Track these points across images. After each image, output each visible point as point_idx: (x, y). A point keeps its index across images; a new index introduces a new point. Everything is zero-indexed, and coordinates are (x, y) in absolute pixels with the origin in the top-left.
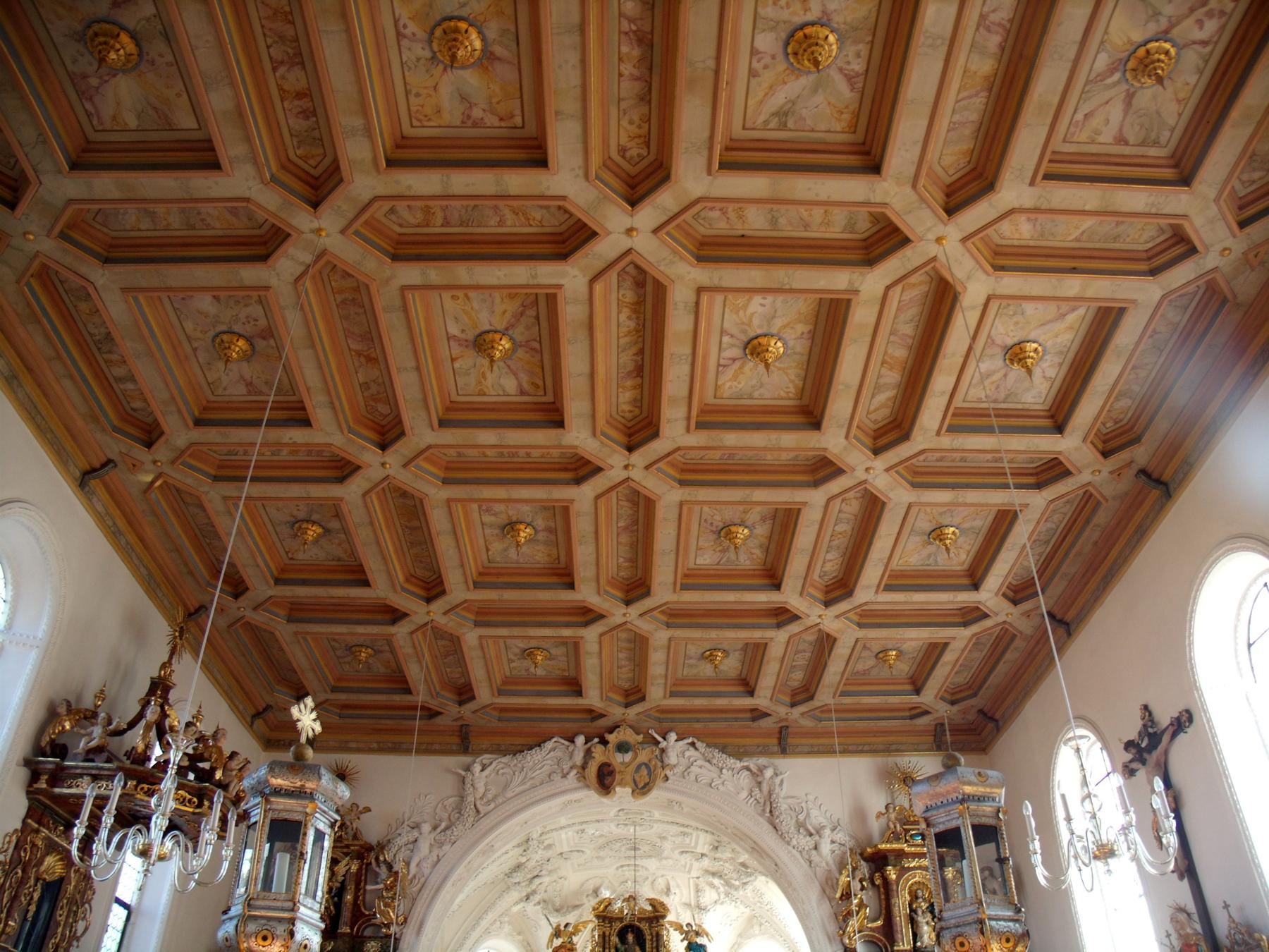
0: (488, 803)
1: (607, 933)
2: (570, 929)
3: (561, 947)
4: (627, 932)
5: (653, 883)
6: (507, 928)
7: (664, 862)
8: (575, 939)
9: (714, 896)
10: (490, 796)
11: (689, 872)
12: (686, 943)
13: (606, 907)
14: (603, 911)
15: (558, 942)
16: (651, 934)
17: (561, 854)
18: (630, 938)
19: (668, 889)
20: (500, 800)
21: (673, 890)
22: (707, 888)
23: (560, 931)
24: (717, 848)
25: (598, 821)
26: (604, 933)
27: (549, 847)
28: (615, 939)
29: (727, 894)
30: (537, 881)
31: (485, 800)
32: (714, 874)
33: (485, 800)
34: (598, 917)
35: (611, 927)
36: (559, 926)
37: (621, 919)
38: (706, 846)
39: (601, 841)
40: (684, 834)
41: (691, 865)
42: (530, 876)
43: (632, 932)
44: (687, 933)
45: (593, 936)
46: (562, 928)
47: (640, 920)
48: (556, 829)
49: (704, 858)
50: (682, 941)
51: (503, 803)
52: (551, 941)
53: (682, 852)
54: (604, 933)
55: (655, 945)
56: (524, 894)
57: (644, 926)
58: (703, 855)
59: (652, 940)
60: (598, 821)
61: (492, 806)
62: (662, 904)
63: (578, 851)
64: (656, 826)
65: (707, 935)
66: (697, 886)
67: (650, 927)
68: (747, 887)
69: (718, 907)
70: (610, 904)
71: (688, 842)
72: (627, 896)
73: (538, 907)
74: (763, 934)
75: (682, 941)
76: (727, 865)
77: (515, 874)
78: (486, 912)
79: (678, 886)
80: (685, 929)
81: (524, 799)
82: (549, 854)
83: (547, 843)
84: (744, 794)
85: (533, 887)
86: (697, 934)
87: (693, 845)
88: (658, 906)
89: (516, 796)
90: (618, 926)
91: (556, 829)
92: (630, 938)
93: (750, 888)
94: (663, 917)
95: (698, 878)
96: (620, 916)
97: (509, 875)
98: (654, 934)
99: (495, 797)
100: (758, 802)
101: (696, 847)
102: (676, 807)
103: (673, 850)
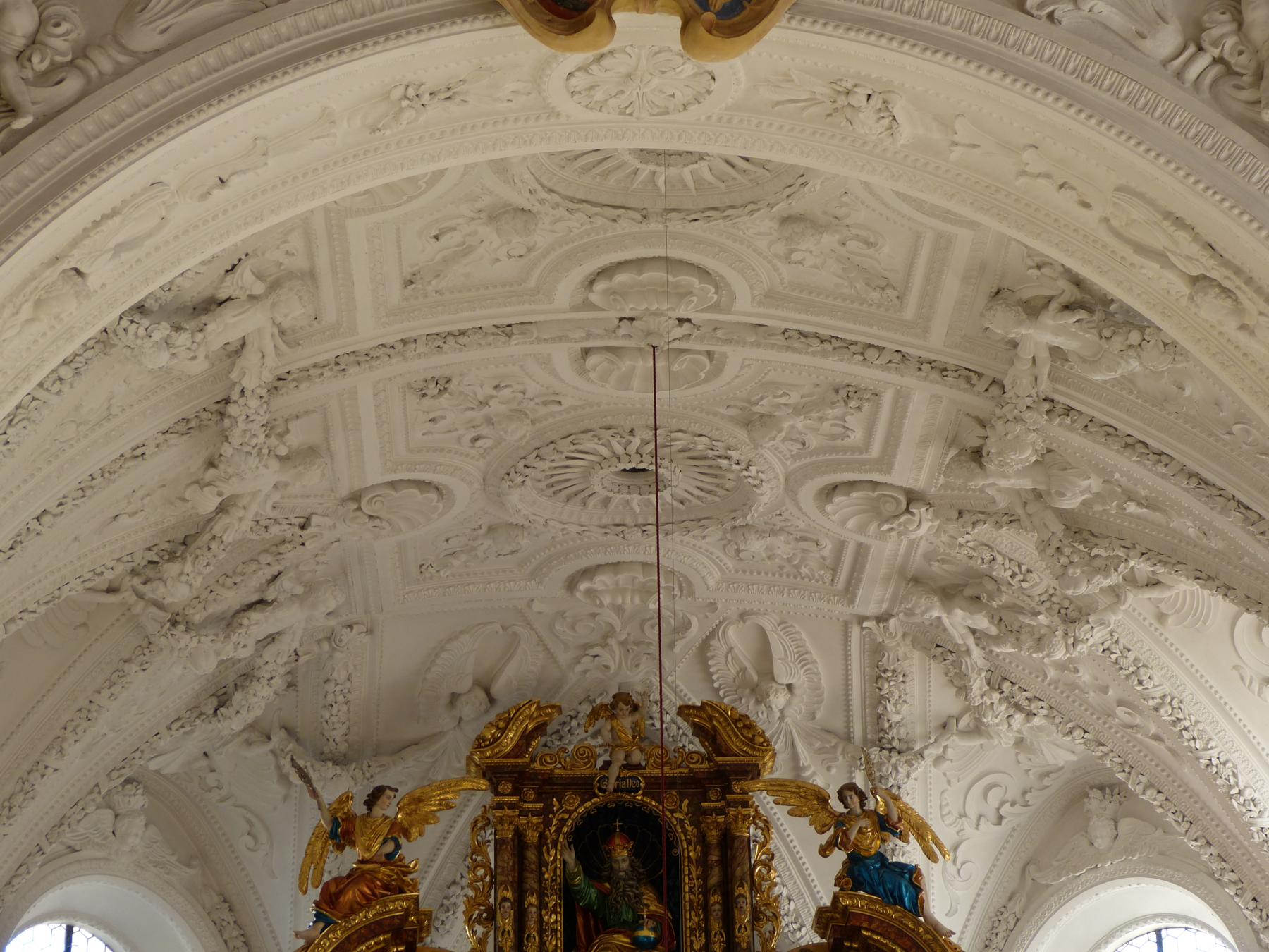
0: (52, 76)
1: (532, 837)
2: (389, 809)
3: (354, 877)
4: (608, 835)
5: (705, 646)
6: (137, 832)
7: (756, 545)
8: (413, 852)
9: (944, 701)
10: (60, 43)
11: (849, 592)
12: (839, 857)
13: (527, 738)
14: (519, 750)
15: (343, 862)
16: (702, 838)
17: (356, 497)
18: (621, 854)
19: (768, 674)
20: (103, 63)
21: (782, 674)
22: (913, 662)
23: (350, 818)
24: (977, 455)
25: (507, 331)
26: (519, 834)
27: (310, 453)
28: (562, 858)
29: (995, 682)
30: (259, 623)
31: (39, 63)
32: (949, 594)
33: (39, 63)
34: (493, 774)
35: (545, 813)
36: (345, 799)
37: (585, 786)
38: (932, 454)
39: (519, 433)
40: (848, 393)
41: (861, 552)
42: (232, 599)
43: (629, 833)
44: (841, 822)
45: (478, 849)
46: (359, 809)
47: (657, 786)
48: (337, 365)
49: (919, 511)
50: (824, 851)
51: (120, 72)
52: (313, 861)
53: (831, 491)
54: (519, 834)
55: (714, 880)
56: (209, 665)
57: (676, 812)
58: (912, 497)
59: (703, 862)
60: (507, 331)
61: (72, 85)
62: (744, 724)
63: (422, 485)
64: (735, 356)
65: (921, 831)
66: (876, 650)
67: (698, 814)
68: (1082, 631)
69: (956, 744)
70: (540, 729)
71: (856, 437)
72: (608, 699)
73: (261, 751)
74: (1129, 851)
75: (824, 851)
76: (1007, 538)
77: (172, 569)
78: (57, 745)
79: (802, 658)
80: (837, 806)
81: (211, 58)
82: (312, 478)
83: (297, 437)
84: (1167, 40)
85: (240, 646)
86: (885, 825)
87: (875, 451)
88: (734, 743)
89: (171, 46)
90: (576, 808)
91: (337, 365)
92: (621, 854)
93: (1094, 636)
94: (751, 771)
95: (882, 619)
96: (580, 771)
97: (149, 569)
98: (713, 836)
99: (82, 52)
100: (1230, 71)
101: (885, 461)
102: (868, 122)
103: (792, 484)
